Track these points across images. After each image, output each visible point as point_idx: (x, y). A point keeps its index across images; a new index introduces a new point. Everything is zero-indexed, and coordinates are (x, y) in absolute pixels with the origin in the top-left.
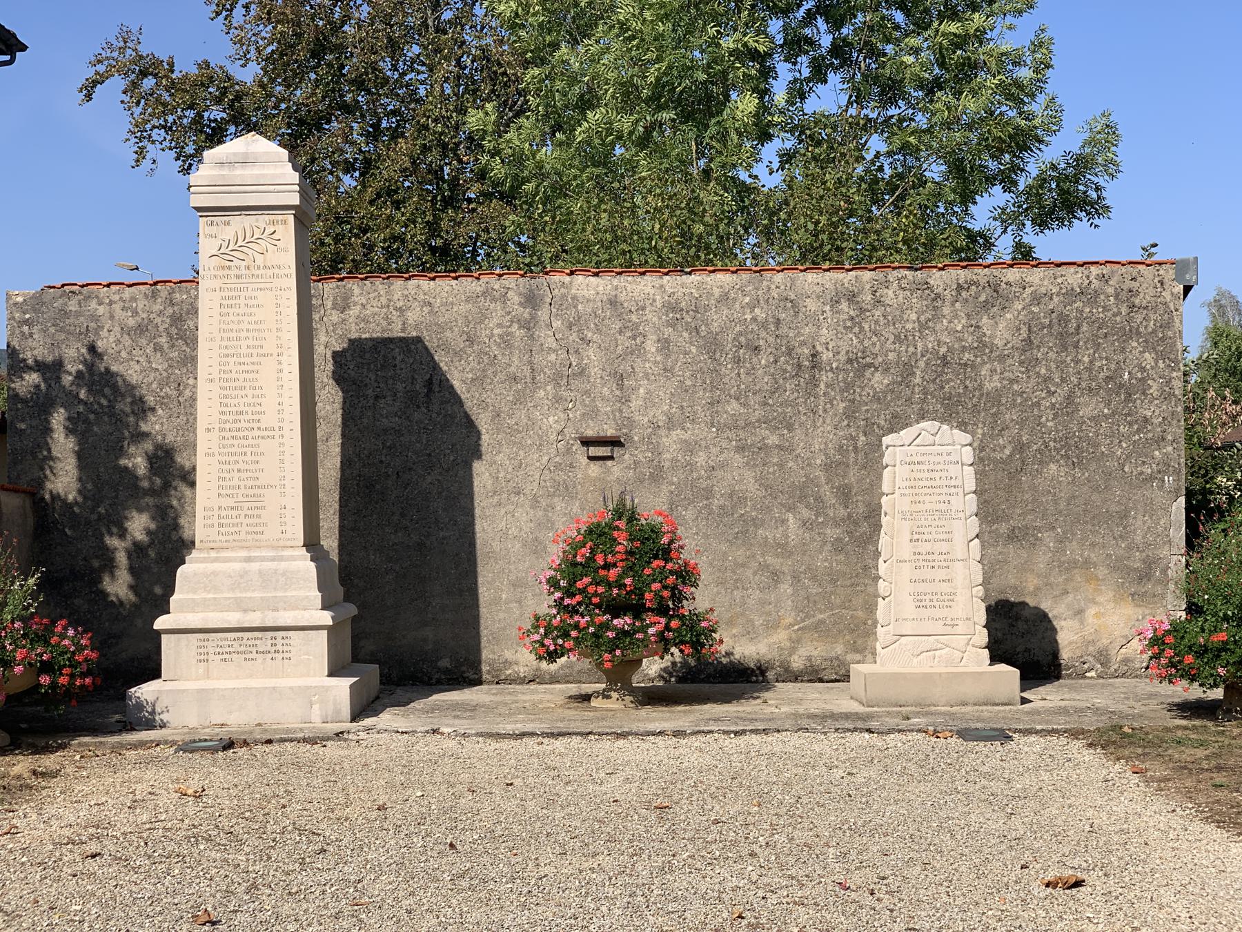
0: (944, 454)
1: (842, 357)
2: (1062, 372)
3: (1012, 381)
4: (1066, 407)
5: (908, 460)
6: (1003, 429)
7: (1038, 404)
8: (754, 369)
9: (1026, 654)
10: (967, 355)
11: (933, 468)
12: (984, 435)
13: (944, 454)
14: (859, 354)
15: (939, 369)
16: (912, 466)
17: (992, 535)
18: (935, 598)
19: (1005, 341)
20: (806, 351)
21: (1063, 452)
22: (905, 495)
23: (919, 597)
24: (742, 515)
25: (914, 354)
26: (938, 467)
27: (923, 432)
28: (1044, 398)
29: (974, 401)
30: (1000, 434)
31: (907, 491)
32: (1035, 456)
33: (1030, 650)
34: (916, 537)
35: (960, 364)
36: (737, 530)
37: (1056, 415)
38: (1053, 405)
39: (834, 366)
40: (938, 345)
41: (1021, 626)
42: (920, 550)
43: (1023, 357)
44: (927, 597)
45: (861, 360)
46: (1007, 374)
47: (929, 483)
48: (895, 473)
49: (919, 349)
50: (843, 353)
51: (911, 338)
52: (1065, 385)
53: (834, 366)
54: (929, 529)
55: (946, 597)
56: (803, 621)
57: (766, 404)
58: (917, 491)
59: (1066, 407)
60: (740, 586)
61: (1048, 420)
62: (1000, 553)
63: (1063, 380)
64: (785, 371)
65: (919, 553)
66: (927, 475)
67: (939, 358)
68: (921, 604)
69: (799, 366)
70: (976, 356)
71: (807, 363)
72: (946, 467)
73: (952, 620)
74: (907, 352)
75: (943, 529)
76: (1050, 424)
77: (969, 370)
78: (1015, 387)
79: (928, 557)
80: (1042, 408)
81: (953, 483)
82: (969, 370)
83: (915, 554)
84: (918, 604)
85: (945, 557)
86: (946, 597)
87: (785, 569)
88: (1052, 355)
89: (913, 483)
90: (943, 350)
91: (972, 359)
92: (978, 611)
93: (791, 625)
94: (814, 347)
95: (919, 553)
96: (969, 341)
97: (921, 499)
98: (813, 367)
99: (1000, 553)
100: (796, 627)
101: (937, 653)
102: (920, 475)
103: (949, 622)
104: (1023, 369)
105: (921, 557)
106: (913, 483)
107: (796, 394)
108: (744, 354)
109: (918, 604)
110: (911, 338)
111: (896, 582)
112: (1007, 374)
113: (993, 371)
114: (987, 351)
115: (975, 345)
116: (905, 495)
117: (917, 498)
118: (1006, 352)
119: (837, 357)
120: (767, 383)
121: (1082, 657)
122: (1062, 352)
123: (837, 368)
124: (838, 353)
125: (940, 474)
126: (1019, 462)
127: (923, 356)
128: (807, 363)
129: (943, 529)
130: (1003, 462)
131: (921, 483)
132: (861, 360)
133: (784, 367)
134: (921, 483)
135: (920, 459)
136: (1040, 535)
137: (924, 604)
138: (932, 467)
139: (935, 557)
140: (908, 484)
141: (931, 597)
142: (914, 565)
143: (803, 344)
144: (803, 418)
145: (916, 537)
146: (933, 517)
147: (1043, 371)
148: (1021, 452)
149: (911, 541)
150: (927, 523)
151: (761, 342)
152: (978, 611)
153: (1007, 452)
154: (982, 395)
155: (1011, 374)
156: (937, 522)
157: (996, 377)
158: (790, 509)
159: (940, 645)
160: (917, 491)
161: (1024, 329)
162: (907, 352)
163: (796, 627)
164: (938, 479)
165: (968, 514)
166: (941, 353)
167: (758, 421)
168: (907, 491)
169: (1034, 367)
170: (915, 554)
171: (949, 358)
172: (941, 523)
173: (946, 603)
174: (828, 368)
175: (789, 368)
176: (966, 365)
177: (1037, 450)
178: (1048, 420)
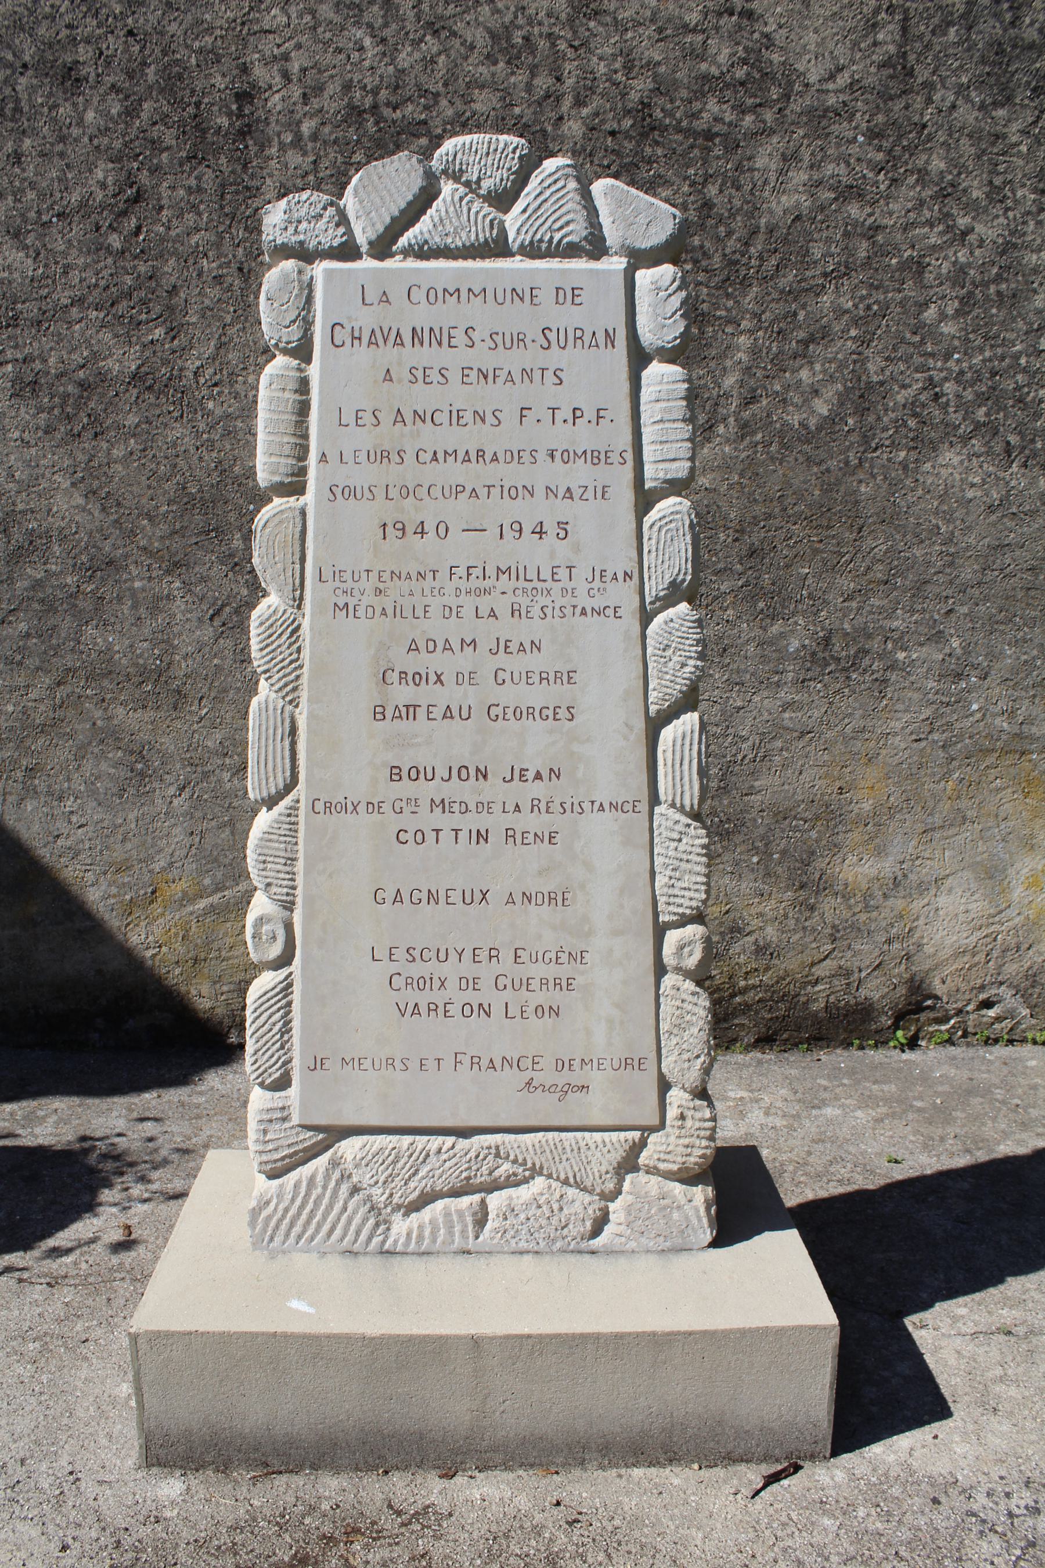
0: (546, 296)
1: (331, 102)
2: (993, 172)
3: (849, 192)
4: (998, 279)
5: (366, 319)
6: (811, 340)
7: (917, 268)
8: (62, 139)
9: (839, 983)
10: (713, 106)
11: (487, 360)
12: (755, 351)
13: (546, 296)
14: (384, 94)
15: (629, 145)
16: (388, 354)
17: (768, 650)
18: (487, 972)
19: (830, 65)
20: (219, 82)
21: (981, 414)
22: (351, 493)
23: (417, 970)
24: (37, 585)
25: (552, 97)
26: (514, 360)
27: (447, 188)
28: (934, 248)
29: (732, 244)
30: (802, 355)
31: (364, 475)
32: (900, 424)
33: (848, 973)
34: (402, 694)
35: (688, 132)
36: (23, 626)
37: (966, 303)
38: (961, 270)
39: (307, 127)
40: (628, 67)
41: (830, 907)
42: (423, 758)
43: (880, 118)
44: (450, 970)
45: (387, 112)
46: (830, 169)
47: (467, 438)
48: (303, 386)
49: (570, 82)
50: (333, 88)
51: (543, 44)
52: (998, 210)
53: (307, 127)
54: (464, 661)
55: (539, 971)
56: (219, 888)
57: (101, 248)
58: (410, 472)
59: (998, 279)
60: (42, 788)
61: (943, 317)
62: (786, 706)
63: (996, 194)
64: (156, 146)
65: (416, 774)
66: (458, 395)
67: (628, 112)
68: (423, 999)
69: (199, 126)
70: (742, 110)
71: (223, 121)
72: (555, 357)
73: (561, 1065)
74: (529, 88)
75: (534, 662)
76: (948, 328)
77: (718, 151)
78: (854, 210)
79: (455, 790)
80: (929, 277)
81: (584, 436)
82: (718, 151)
83: (395, 773)
84: (412, 996)
85: (538, 790)
86: (539, 971)
87: (167, 742)
88: (967, 115)
89: (388, 435)
90: (640, 86)
91: (729, 117)
92: (680, 1027)
93: (188, 898)
94: (245, 69)
95: (416, 774)
96: (723, 58)
97: (430, 512)
98: (243, 133)
99: (786, 706)
100: (202, 904)
101: (495, 1201)
102: (424, 398)
103: (546, 1076)
104: (880, 156)
105: (426, 790)
106: (388, 435)
107: (190, 218)
108: (32, 90)
109: (412, 996)
110: (543, 44)
111: (309, 900)
112: (830, 169)
113: (790, 158)
114: (775, 93)
115: (740, 73)
116: (351, 493)
117: (410, 512)
118: (831, 101)
119: (316, 103)
120: (103, 185)
121: (982, 988)
122: (995, 104)
123: (315, 137)
124: (319, 89)
125: (523, 392)
126: (854, 438)
127: (579, 102)
128: (223, 121)
129: (534, 662)
130: (807, 436)
131: (430, 437)
132: (387, 112)
133: (155, 132)
134: (430, 437)
135: (423, 316)
136: (901, 655)
137: (439, 997)
138: (483, 357)
139: (494, 789)
140: (364, 439)
141: (467, 969)
142: (394, 823)
143: (212, 57)
144: (214, 293)
145: (402, 694)
146: (485, 604)
147: (937, 164)
148: (862, 412)
149: (379, 713)
150: (453, 630)
151: (84, 53)
152: (680, 1027)
153: (822, 408)
154: (755, 232)
155: (842, 169)
156: (506, 628)
157: (799, 177)
158: (175, 567)
159: (505, 1168)
160: (410, 472)
161: (887, 35)
162: (529, 88)
163: (202, 904)
164: (511, 416)
165: (654, 587)
166: (634, 96)
167: (78, 301)
168: (364, 475)
169: (911, 150)
170: (395, 773)
171: (658, 114)
172: (522, 631)
173: (540, 997)
174: (288, 138)
175: (169, 138)
176: (709, 135)
177: (913, 407)
178: (943, 317)
